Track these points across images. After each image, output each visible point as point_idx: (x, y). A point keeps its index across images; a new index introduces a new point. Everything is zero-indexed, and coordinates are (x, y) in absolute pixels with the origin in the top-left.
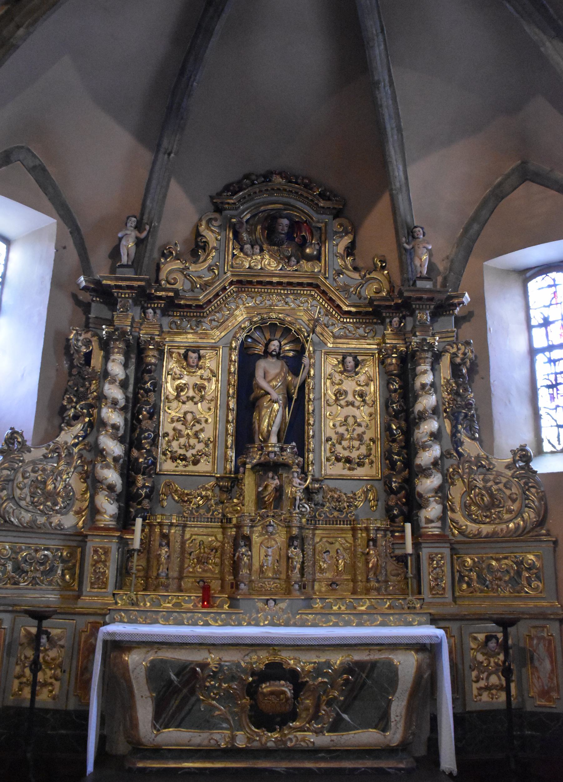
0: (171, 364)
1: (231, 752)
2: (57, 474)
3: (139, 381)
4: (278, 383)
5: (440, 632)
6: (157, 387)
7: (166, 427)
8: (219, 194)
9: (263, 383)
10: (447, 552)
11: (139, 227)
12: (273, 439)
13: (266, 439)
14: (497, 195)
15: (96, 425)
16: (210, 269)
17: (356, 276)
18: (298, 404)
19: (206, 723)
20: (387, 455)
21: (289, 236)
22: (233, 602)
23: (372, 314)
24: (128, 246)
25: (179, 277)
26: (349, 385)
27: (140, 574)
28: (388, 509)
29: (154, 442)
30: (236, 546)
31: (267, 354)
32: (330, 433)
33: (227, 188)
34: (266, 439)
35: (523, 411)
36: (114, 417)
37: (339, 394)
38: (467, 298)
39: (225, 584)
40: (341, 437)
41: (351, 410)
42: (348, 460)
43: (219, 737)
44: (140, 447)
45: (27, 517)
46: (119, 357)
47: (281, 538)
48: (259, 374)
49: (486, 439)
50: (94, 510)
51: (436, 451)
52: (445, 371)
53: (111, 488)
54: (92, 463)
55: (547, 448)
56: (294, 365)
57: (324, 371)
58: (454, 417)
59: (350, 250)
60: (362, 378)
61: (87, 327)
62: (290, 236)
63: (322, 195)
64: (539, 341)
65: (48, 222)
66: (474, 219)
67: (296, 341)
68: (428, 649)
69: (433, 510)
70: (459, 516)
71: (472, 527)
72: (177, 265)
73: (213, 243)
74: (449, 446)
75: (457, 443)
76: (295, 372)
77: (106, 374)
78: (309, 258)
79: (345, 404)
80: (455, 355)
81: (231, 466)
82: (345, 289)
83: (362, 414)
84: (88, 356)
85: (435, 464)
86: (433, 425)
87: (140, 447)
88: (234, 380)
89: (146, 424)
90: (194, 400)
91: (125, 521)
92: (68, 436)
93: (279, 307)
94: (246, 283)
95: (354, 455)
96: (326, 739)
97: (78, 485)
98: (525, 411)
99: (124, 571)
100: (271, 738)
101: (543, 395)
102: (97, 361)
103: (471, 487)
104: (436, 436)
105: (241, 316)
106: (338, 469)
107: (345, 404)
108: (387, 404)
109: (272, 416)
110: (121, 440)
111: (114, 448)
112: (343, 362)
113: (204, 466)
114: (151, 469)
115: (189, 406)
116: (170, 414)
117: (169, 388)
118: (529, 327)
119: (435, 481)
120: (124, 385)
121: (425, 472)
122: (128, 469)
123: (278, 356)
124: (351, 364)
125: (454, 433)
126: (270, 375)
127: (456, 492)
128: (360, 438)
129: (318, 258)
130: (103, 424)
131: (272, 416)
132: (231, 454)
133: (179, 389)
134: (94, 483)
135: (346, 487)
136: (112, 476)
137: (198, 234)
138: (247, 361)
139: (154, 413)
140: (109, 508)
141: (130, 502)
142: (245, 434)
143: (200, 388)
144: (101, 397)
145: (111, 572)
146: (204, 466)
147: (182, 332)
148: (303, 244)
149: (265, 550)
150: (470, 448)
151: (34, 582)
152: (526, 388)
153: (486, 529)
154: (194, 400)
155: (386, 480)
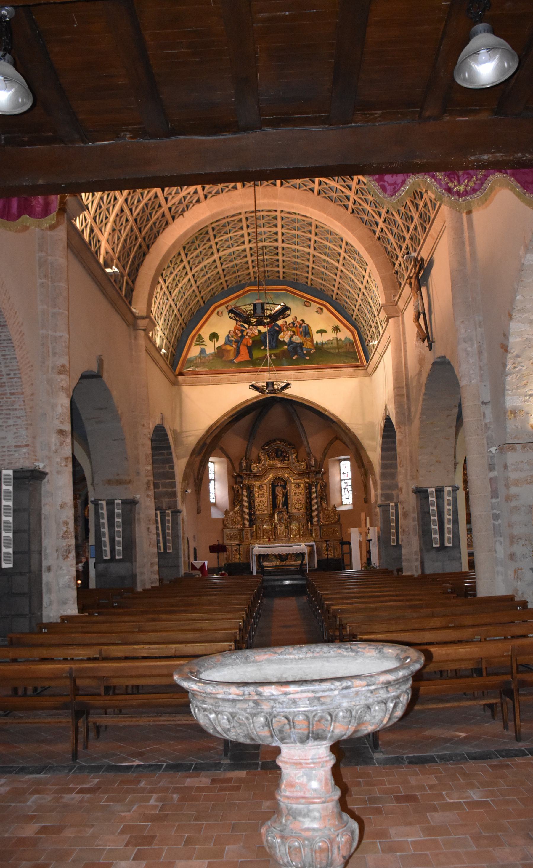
0: (256, 489)
1: (276, 566)
2: (236, 518)
3: (250, 496)
4: (281, 492)
5: (314, 543)
6: (254, 495)
7: (256, 504)
8: (263, 446)
9: (277, 493)
10: (318, 528)
11: (246, 459)
12: (281, 506)
13: (279, 507)
14: (331, 442)
15: (242, 506)
16: (263, 465)
17: (298, 464)
18: (286, 496)
19: (272, 561)
20: (306, 507)
21: (280, 455)
22: (275, 540)
23: (302, 474)
24: (244, 464)
25: (256, 468)
26: (298, 491)
27: (256, 537)
28: (307, 519)
29: (254, 508)
30: (274, 529)
31: (278, 485)
32: (294, 503)
33: (265, 444)
34: (279, 503)
35: (338, 495)
36: (246, 504)
37: (295, 493)
38: (323, 470)
39: (273, 535)
40: (296, 503)
41: (298, 497)
42: (298, 509)
43: (274, 564)
44: (252, 510)
45: (231, 527)
46: (245, 490)
47: (283, 527)
48: (276, 490)
49: (328, 503)
50: (244, 524)
51: (316, 506)
52: (319, 488)
53: (247, 519)
54: (242, 514)
55: (343, 503)
56: (284, 487)
57: (292, 487)
58: (322, 498)
59: (297, 457)
60: (301, 489)
61: (236, 483)
62: (281, 455)
63: (289, 445)
64: (342, 478)
65: (225, 460)
66: (325, 449)
67: (284, 481)
68: (312, 546)
69: (316, 519)
70: (322, 520)
71: (325, 523)
72: (255, 465)
73: (263, 458)
74: (319, 504)
75: (322, 504)
76: (285, 489)
77: (242, 494)
78: (286, 460)
79: (296, 495)
80: (320, 484)
81: (271, 512)
82: (296, 467)
83: (301, 497)
84: (238, 490)
85: (316, 509)
86: (315, 501)
87: (252, 510)
88: (271, 492)
89: (253, 504)
90: (262, 498)
91: (251, 526)
92: (236, 509)
93: (280, 474)
94: (273, 468)
95: (299, 507)
96: (294, 563)
97: (240, 519)
98: (339, 495)
99: (252, 536)
100: (283, 563)
101: (343, 490)
102: (240, 491)
103: (324, 514)
104: (316, 503)
105: (271, 476)
106: (295, 511)
107: (296, 495)
108: (306, 495)
109: (280, 500)
110: (248, 509)
111: (247, 511)
112: (296, 486)
113: (266, 512)
114: (254, 514)
115: (261, 499)
116: (257, 501)
117: (256, 495)
118: (340, 474)
119: (316, 513)
120: (247, 497)
121: (314, 511)
122: (250, 514)
123: (281, 486)
124: (298, 485)
125: (321, 502)
126: (279, 491)
127: (321, 515)
128: (300, 503)
129: (289, 460)
130: (244, 506)
131: (280, 500)
132: (272, 509)
133: (259, 495)
134: (243, 519)
135: (297, 515)
136: (247, 517)
137: (259, 457)
138: (274, 486)
139: (254, 502)
140: (247, 523)
141: (252, 522)
142: (274, 505)
143: (263, 494)
144: (242, 500)
145: (249, 536)
146: (266, 512)
147: (258, 481)
148: (285, 457)
149: (281, 529)
150: (324, 505)
151: (234, 540)
152: (339, 489)
153: (327, 523)
154: (262, 498)
155: (306, 513)
